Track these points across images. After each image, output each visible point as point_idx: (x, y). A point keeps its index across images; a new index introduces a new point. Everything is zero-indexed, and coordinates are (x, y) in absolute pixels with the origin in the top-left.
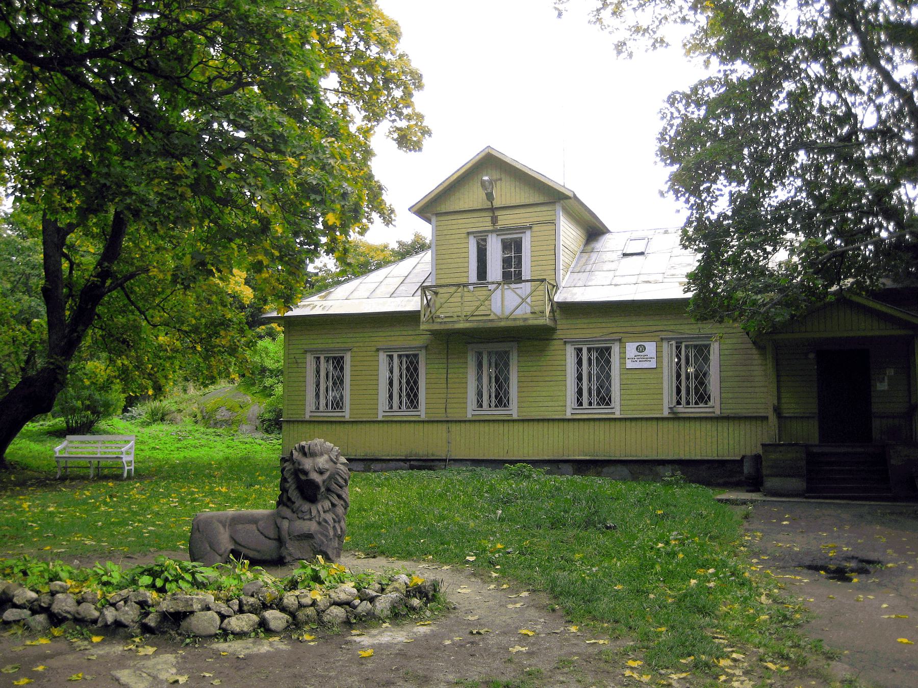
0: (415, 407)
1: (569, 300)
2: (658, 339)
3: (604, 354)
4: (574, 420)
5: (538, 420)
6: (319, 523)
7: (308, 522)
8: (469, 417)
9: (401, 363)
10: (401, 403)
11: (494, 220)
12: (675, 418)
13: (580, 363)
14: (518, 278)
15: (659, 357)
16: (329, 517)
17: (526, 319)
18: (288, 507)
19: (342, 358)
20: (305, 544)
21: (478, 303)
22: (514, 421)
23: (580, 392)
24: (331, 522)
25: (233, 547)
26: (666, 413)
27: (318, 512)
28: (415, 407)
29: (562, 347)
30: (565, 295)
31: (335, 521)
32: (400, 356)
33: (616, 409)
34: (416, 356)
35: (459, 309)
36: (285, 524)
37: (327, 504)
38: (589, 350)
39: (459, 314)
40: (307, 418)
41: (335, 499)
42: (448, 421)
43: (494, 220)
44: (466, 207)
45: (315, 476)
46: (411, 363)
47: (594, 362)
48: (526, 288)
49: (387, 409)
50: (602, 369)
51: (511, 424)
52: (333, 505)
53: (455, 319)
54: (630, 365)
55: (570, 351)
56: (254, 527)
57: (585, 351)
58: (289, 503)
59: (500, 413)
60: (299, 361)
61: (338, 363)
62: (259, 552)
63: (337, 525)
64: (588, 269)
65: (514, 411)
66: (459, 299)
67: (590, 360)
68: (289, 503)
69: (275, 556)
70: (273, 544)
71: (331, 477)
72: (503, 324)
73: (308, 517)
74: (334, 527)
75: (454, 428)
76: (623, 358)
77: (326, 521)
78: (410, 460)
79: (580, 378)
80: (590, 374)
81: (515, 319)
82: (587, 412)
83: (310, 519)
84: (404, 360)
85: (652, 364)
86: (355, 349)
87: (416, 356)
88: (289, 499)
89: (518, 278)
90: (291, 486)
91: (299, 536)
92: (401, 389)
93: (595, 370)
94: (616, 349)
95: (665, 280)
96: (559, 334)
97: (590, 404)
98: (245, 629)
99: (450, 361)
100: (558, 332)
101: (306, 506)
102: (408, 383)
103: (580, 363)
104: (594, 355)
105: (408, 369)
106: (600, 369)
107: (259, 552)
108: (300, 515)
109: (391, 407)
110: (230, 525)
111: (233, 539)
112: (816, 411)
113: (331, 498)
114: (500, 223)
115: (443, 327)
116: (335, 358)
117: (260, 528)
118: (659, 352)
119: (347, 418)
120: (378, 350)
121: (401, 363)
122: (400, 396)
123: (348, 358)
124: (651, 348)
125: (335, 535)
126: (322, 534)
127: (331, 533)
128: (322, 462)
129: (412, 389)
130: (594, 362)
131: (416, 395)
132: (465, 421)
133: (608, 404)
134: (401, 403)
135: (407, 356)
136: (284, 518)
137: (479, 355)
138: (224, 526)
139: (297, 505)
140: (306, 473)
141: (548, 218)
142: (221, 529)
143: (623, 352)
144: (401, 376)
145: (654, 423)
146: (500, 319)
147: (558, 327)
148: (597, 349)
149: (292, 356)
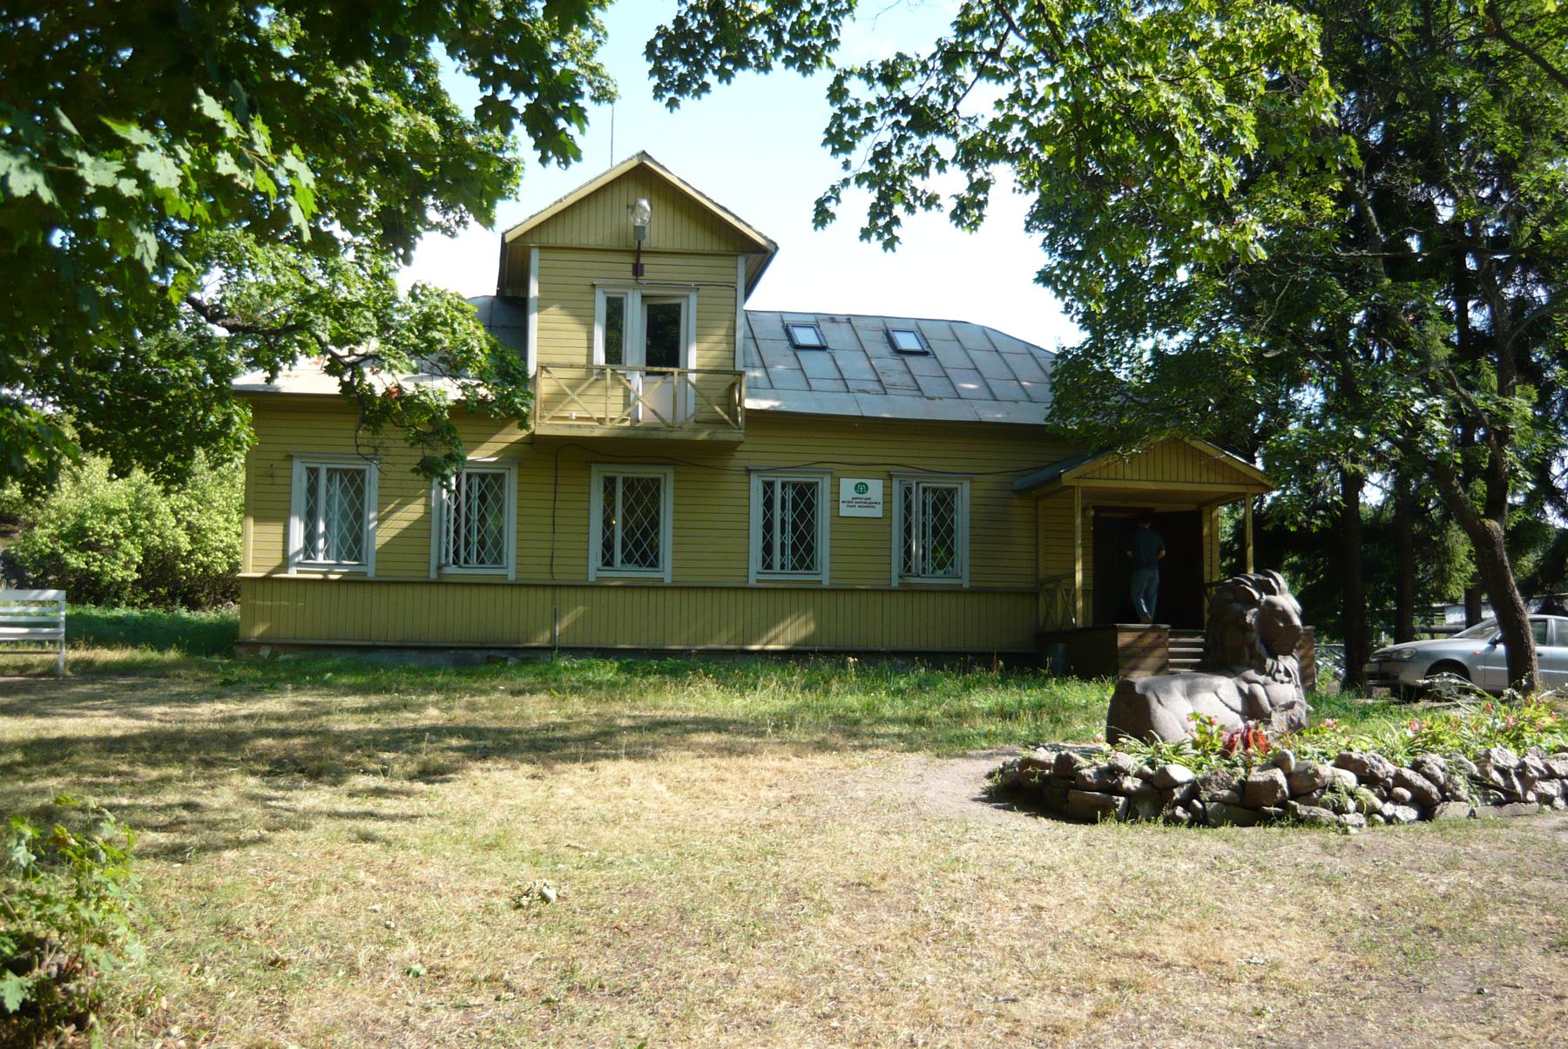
4: (760, 589)
5: (704, 588)
11: (638, 270)
12: (906, 590)
15: (887, 502)
22: (665, 588)
26: (895, 583)
29: (745, 479)
33: (824, 574)
38: (784, 486)
42: (554, 587)
43: (638, 270)
44: (584, 241)
51: (661, 593)
54: (844, 511)
59: (802, 577)
65: (666, 572)
79: (768, 527)
82: (778, 576)
85: (877, 512)
94: (825, 485)
96: (739, 460)
97: (783, 566)
114: (646, 275)
116: (345, 472)
118: (888, 495)
124: (876, 488)
132: (585, 587)
133: (808, 568)
137: (609, 484)
141: (727, 279)
145: (879, 597)
148: (794, 485)
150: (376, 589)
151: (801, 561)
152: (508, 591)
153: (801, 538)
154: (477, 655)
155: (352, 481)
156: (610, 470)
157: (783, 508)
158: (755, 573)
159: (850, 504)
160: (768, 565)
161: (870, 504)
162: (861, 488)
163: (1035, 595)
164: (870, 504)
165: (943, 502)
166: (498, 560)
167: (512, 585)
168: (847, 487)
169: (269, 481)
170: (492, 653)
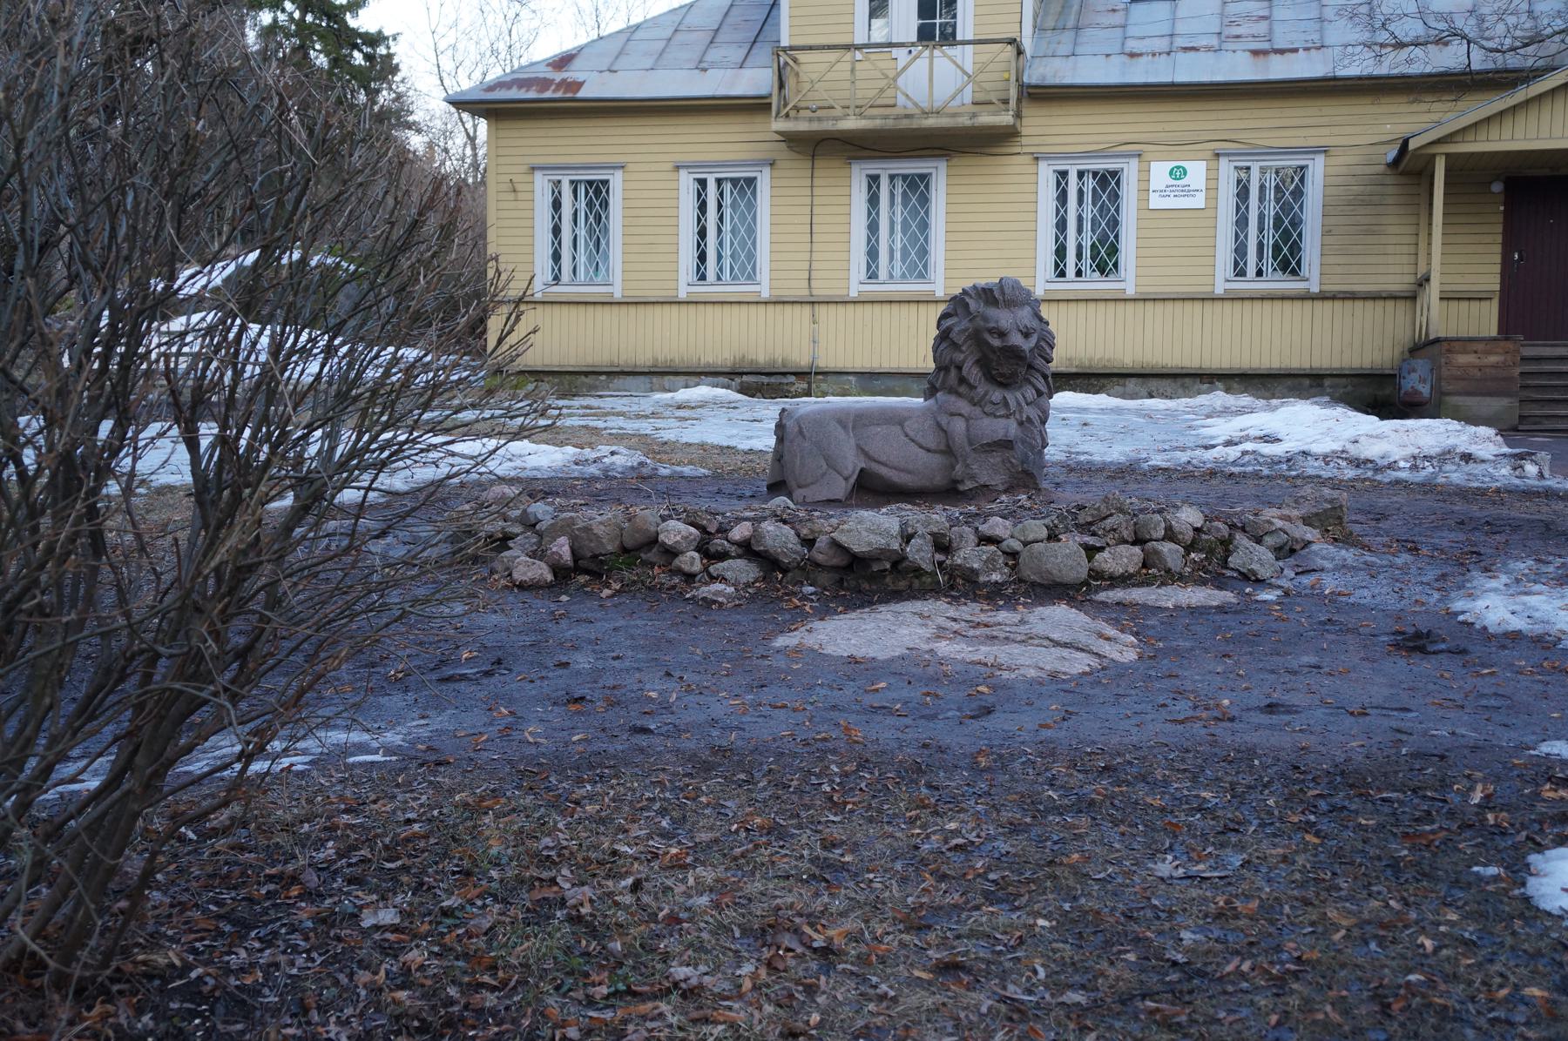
1: (1050, 81)
2: (1209, 154)
3: (1108, 182)
6: (1021, 424)
7: (1003, 421)
8: (853, 294)
13: (1062, 198)
14: (949, 38)
15: (1212, 189)
17: (974, 115)
18: (959, 395)
19: (605, 183)
21: (882, 84)
23: (1061, 252)
27: (1019, 404)
30: (1041, 70)
35: (847, 94)
36: (959, 426)
38: (1081, 174)
39: (846, 103)
45: (1016, 339)
47: (1088, 198)
48: (966, 56)
50: (913, 240)
53: (838, 112)
54: (1156, 202)
55: (1046, 175)
56: (896, 429)
57: (1073, 178)
58: (962, 389)
60: (519, 187)
61: (598, 192)
64: (1071, 23)
66: (848, 75)
67: (1081, 193)
69: (939, 480)
70: (936, 460)
72: (931, 122)
73: (1002, 412)
75: (822, 310)
76: (1145, 191)
78: (742, 374)
80: (1080, 219)
81: (954, 115)
83: (1007, 417)
85: (1199, 201)
86: (630, 167)
87: (751, 182)
89: (949, 38)
91: (988, 444)
93: (1089, 211)
94: (1130, 172)
95: (1225, 46)
98: (1131, 571)
99: (817, 191)
100: (1024, 141)
101: (997, 395)
103: (1062, 198)
104: (1090, 183)
106: (1101, 210)
107: (909, 472)
111: (861, 450)
112: (1498, 287)
115: (815, 126)
117: (911, 434)
120: (677, 168)
123: (616, 181)
124: (1197, 171)
126: (1023, 442)
130: (1088, 198)
136: (952, 415)
137: (874, 180)
138: (845, 427)
139: (981, 390)
143: (1144, 179)
146: (926, 114)
147: (1024, 131)
149: (507, 178)
150: (624, 308)
151: (912, 268)
152: (762, 308)
153: (1286, 235)
155: (598, 192)
156: (873, 167)
157: (1261, 199)
158: (1222, 279)
159: (1163, 194)
160: (872, 275)
161: (1188, 192)
162: (1178, 173)
163: (1413, 298)
164: (1188, 192)
165: (1290, 191)
166: (751, 277)
168: (1160, 172)
169: (512, 196)
170: (745, 378)
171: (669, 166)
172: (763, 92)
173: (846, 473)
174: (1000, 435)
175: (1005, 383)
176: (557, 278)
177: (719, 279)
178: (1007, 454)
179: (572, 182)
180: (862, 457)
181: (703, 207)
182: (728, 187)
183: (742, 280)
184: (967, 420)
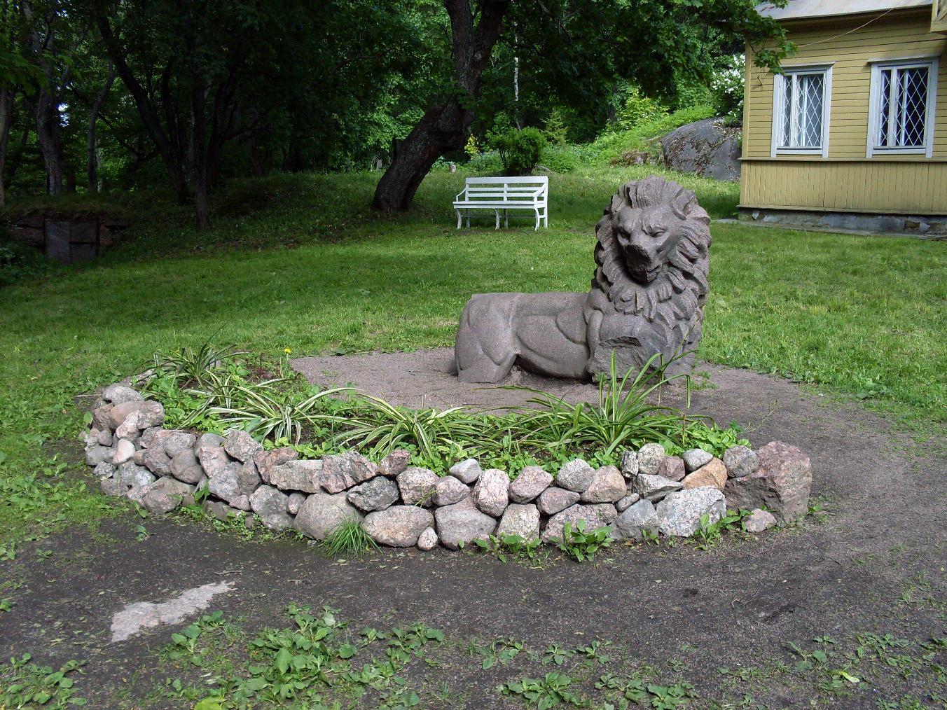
0: (919, 143)
6: (650, 321)
9: (902, 82)
10: (899, 137)
16: (668, 310)
20: (626, 353)
24: (671, 319)
25: (518, 352)
28: (919, 143)
31: (678, 318)
32: (901, 72)
34: (924, 71)
36: (598, 319)
37: (666, 289)
40: (774, 157)
41: (679, 280)
46: (917, 80)
49: (880, 144)
52: (677, 290)
58: (604, 285)
62: (556, 362)
63: (682, 324)
68: (604, 285)
71: (672, 242)
74: (676, 327)
77: (662, 318)
83: (635, 314)
84: (907, 76)
86: (837, 64)
88: (604, 278)
90: (608, 254)
92: (900, 118)
101: (630, 290)
102: (910, 108)
105: (911, 89)
108: (618, 305)
109: (885, 143)
110: (517, 316)
111: (518, 337)
113: (672, 277)
116: (812, 77)
117: (560, 323)
119: (826, 157)
120: (870, 64)
121: (902, 82)
122: (899, 128)
123: (829, 76)
125: (678, 340)
126: (654, 338)
127: (670, 337)
128: (655, 217)
129: (915, 118)
131: (920, 127)
134: (899, 137)
135: (912, 71)
136: (595, 309)
140: (628, 236)
142: (502, 324)
144: (901, 99)
154: (898, 220)
167: (929, 163)
170: (909, 219)
171: (864, 63)
172: (929, 3)
173: (498, 359)
174: (626, 332)
175: (641, 280)
176: (787, 143)
177: (897, 144)
178: (636, 350)
179: (799, 77)
180: (518, 345)
181: (887, 92)
182: (907, 76)
183: (913, 146)
184: (604, 315)
